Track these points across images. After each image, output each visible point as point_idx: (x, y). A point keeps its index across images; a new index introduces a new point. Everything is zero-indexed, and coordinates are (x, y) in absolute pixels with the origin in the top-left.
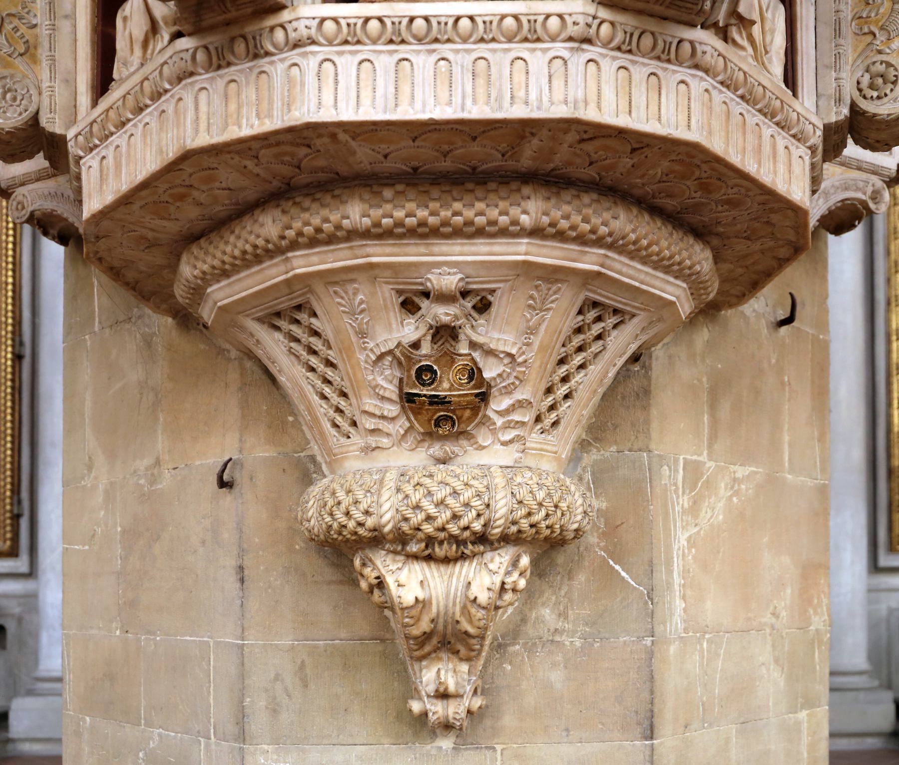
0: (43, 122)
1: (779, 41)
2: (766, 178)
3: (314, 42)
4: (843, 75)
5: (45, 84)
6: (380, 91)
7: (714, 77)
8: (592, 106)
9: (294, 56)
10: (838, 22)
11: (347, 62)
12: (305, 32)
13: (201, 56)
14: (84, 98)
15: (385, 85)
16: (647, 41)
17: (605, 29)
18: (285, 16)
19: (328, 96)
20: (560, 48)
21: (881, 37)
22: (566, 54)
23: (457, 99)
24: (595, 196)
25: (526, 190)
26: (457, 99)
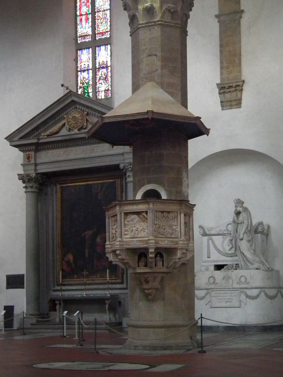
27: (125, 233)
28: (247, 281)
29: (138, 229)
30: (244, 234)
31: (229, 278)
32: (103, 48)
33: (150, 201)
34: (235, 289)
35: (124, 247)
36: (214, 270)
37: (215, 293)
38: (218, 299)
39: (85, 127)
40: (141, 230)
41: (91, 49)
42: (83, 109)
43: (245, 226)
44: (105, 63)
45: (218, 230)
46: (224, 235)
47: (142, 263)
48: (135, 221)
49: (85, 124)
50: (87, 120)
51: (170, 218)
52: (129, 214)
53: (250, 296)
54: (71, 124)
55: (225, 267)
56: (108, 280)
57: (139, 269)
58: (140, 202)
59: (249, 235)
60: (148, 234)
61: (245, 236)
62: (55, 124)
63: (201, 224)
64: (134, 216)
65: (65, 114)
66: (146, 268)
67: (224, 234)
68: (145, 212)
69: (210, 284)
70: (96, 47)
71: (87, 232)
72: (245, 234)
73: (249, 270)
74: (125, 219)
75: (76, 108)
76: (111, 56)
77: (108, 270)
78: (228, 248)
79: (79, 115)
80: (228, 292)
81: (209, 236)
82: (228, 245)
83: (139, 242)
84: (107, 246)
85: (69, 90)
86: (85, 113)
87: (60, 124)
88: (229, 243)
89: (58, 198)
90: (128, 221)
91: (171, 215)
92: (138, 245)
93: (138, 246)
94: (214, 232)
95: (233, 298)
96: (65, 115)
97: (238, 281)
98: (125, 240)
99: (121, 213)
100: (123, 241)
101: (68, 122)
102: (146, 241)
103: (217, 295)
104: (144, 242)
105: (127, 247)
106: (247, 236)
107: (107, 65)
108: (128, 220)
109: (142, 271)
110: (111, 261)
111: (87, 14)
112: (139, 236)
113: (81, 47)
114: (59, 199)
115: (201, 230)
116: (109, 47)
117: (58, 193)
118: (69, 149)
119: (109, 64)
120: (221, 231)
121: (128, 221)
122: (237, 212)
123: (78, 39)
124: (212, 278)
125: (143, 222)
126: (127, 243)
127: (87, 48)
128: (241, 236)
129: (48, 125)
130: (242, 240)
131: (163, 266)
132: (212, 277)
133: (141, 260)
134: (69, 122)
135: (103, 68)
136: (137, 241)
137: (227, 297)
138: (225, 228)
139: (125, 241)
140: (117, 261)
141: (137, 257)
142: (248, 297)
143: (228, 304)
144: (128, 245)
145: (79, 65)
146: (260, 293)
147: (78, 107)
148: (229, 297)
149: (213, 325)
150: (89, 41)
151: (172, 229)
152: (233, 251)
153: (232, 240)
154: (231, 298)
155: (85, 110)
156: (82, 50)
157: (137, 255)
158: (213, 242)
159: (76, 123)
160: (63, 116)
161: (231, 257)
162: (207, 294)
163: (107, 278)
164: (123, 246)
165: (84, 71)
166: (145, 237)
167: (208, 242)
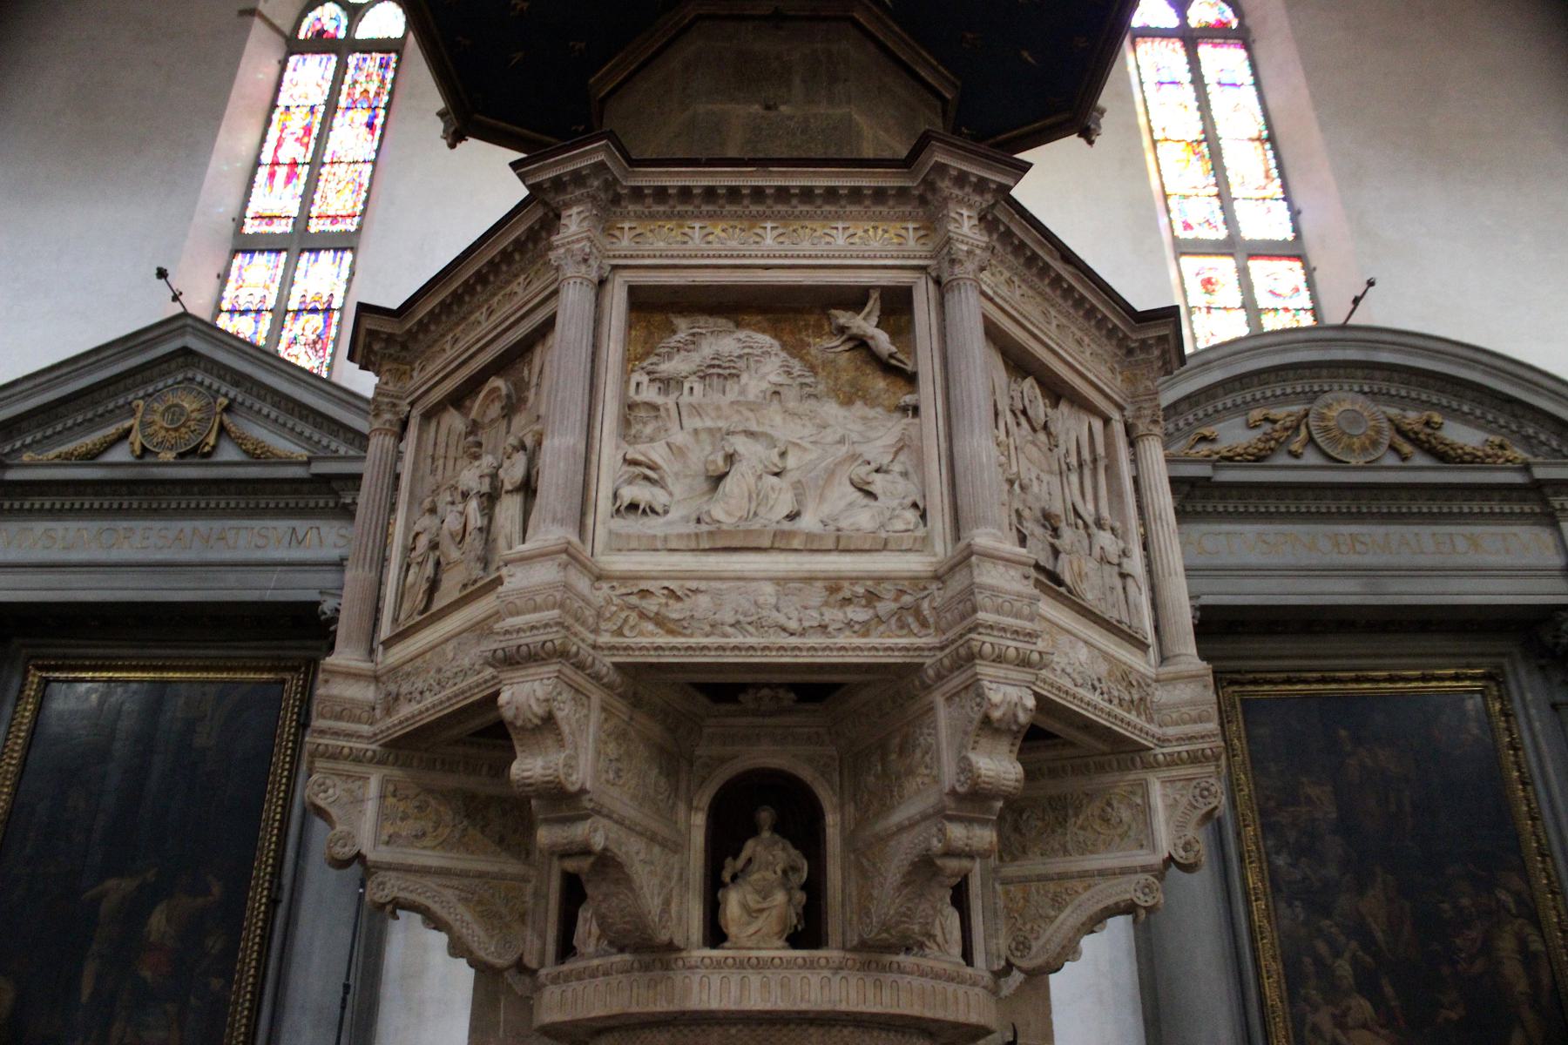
0: (526, 960)
1: (956, 934)
2: (951, 1017)
3: (697, 967)
4: (1001, 941)
5: (529, 938)
6: (733, 994)
7: (911, 973)
8: (844, 1003)
9: (687, 973)
10: (995, 909)
11: (715, 979)
12: (693, 963)
13: (636, 965)
14: (551, 949)
15: (735, 991)
16: (873, 965)
17: (850, 963)
18: (684, 954)
19: (705, 997)
20: (826, 973)
21: (1020, 921)
22: (830, 975)
23: (773, 999)
24: (851, 1029)
25: (811, 1030)
26: (773, 999)
27: (628, 493)
29: (791, 461)
32: (327, 257)
33: (961, 179)
35: (605, 639)
39: (207, 449)
40: (831, 473)
41: (284, 255)
42: (215, 386)
44: (325, 299)
47: (765, 894)
48: (754, 384)
49: (212, 440)
50: (222, 429)
51: (1062, 449)
52: (682, 323)
54: (155, 434)
57: (719, 965)
58: (831, 194)
60: (923, 516)
62: (91, 425)
64: (742, 334)
65: (141, 393)
66: (810, 965)
68: (873, 305)
70: (302, 251)
74: (631, 361)
75: (192, 380)
76: (349, 281)
79: (195, 406)
83: (816, 595)
84: (332, 690)
85: (176, 309)
86: (224, 401)
87: (111, 430)
89: (21, 723)
90: (667, 384)
91: (1071, 426)
92: (793, 625)
93: (794, 641)
96: (142, 398)
98: (620, 563)
99: (602, 283)
100: (599, 578)
101: (145, 425)
102: (903, 592)
104: (872, 598)
105: (644, 641)
107: (330, 303)
108: (667, 367)
109: (757, 995)
110: (359, 857)
111: (294, 164)
112: (808, 522)
113: (246, 246)
114: (24, 728)
116: (348, 256)
117: (27, 703)
118: (122, 525)
119: (336, 304)
121: (667, 384)
123: (248, 221)
125: (848, 402)
126: (651, 606)
127: (270, 251)
129: (59, 427)
131: (967, 956)
133: (740, 862)
134: (153, 423)
135: (314, 311)
136: (780, 581)
139: (625, 578)
140: (425, 871)
141: (699, 820)
144: (650, 627)
145: (229, 292)
147: (199, 378)
150: (284, 234)
151: (1097, 551)
155: (223, 390)
156: (252, 252)
157: (704, 799)
159: (176, 430)
160: (130, 403)
164: (596, 631)
165: (244, 313)
166: (884, 547)
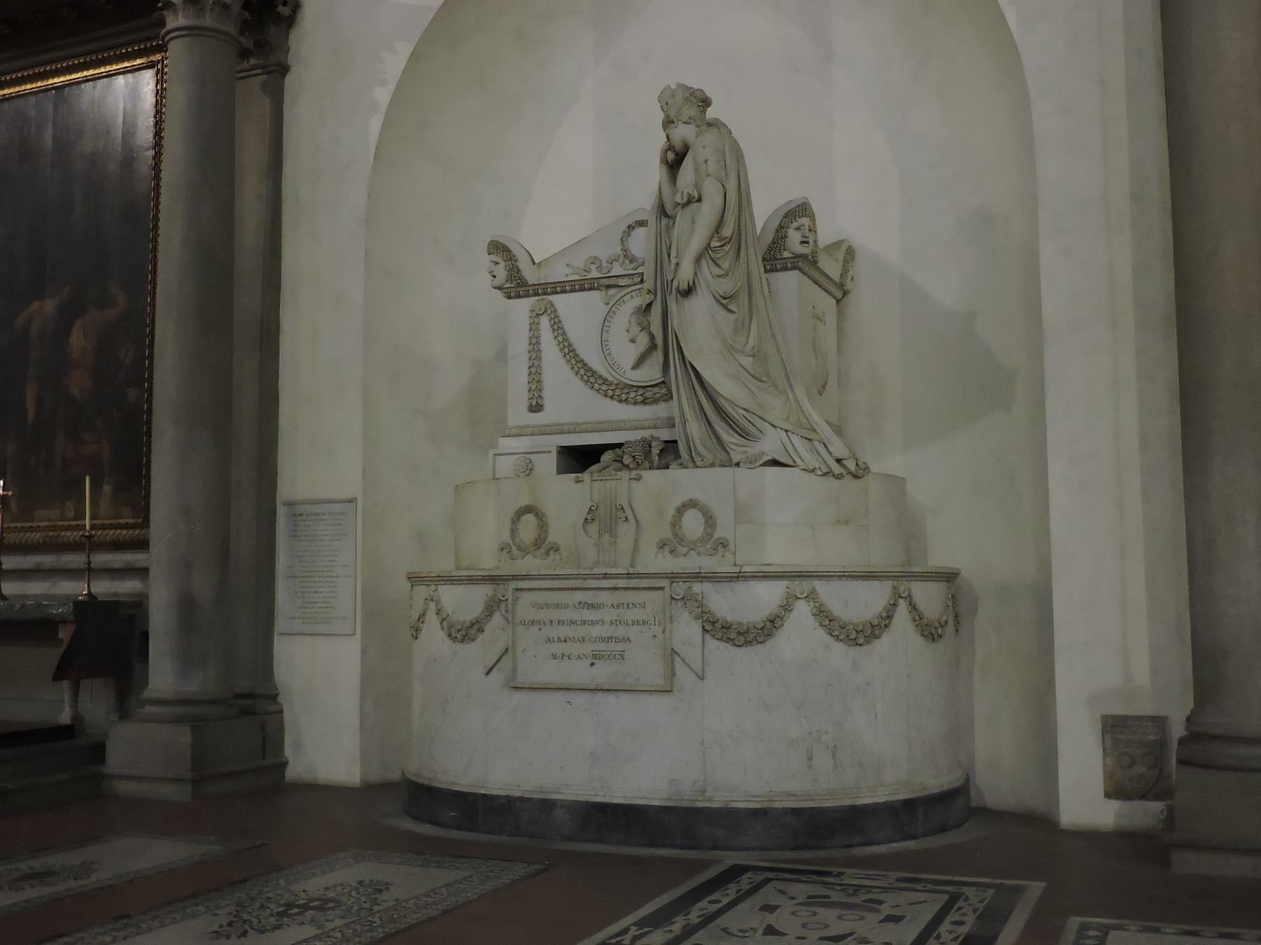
28: (716, 535)
30: (698, 261)
31: (620, 514)
34: (645, 583)
36: (558, 473)
37: (535, 605)
38: (549, 640)
43: (706, 214)
45: (580, 262)
46: (608, 287)
53: (727, 627)
55: (607, 457)
56: (88, 527)
59: (726, 265)
61: (707, 268)
63: (505, 236)
67: (612, 281)
69: (519, 548)
71: (35, 306)
72: (703, 263)
73: (729, 471)
77: (88, 479)
78: (625, 351)
80: (604, 597)
81: (536, 294)
82: (633, 341)
88: (635, 329)
94: (560, 273)
95: (633, 632)
97: (667, 533)
103: (543, 615)
106: (716, 271)
115: (497, 263)
120: (593, 266)
122: (677, 154)
124: (529, 518)
128: (686, 273)
130: (688, 292)
132: (528, 509)
137: (596, 631)
138: (618, 250)
142: (717, 629)
143: (603, 673)
146: (787, 607)
148: (607, 631)
149: (517, 794)
152: (650, 373)
153: (649, 305)
154: (621, 632)
158: (557, 326)
161: (644, 402)
162: (493, 606)
163: (85, 519)
167: (534, 327)
